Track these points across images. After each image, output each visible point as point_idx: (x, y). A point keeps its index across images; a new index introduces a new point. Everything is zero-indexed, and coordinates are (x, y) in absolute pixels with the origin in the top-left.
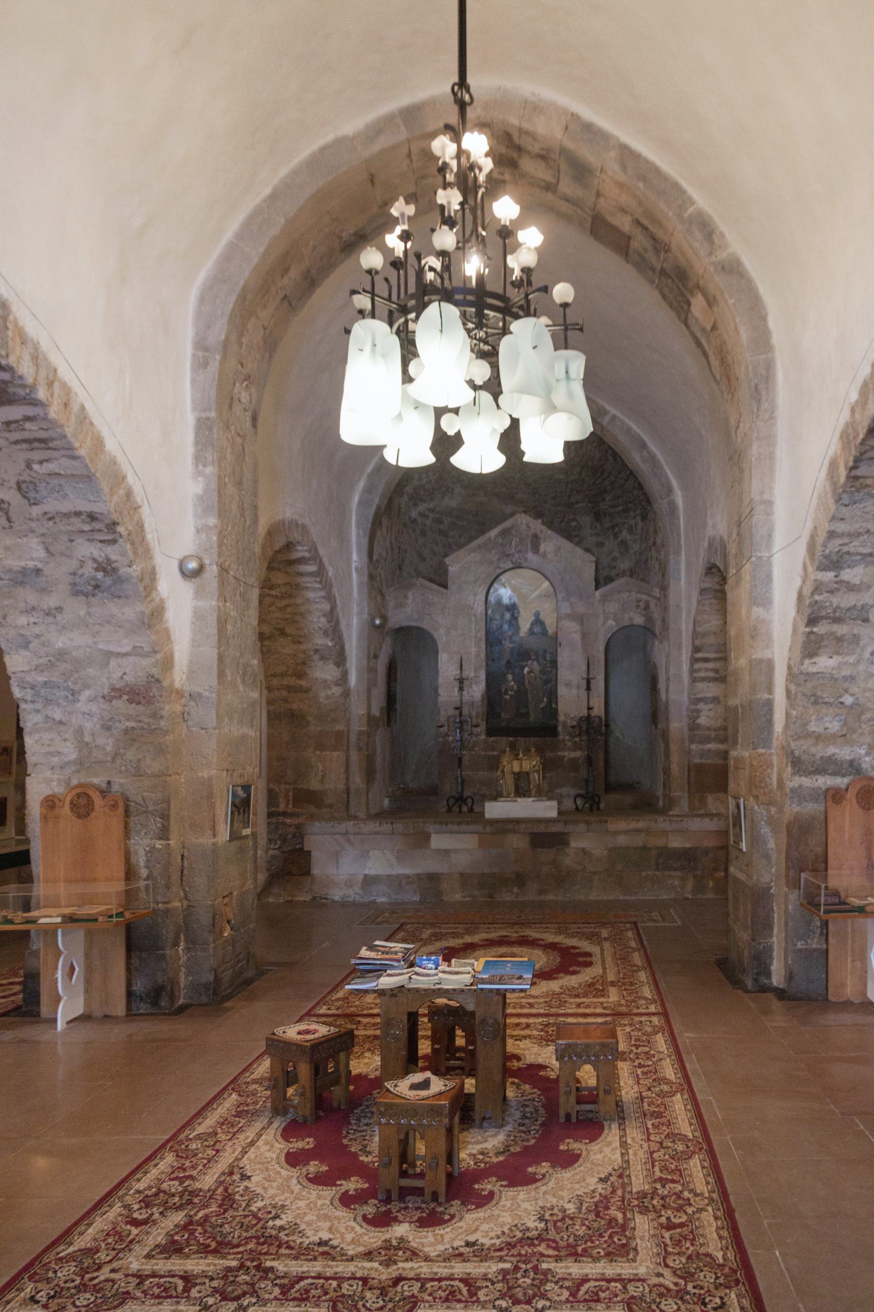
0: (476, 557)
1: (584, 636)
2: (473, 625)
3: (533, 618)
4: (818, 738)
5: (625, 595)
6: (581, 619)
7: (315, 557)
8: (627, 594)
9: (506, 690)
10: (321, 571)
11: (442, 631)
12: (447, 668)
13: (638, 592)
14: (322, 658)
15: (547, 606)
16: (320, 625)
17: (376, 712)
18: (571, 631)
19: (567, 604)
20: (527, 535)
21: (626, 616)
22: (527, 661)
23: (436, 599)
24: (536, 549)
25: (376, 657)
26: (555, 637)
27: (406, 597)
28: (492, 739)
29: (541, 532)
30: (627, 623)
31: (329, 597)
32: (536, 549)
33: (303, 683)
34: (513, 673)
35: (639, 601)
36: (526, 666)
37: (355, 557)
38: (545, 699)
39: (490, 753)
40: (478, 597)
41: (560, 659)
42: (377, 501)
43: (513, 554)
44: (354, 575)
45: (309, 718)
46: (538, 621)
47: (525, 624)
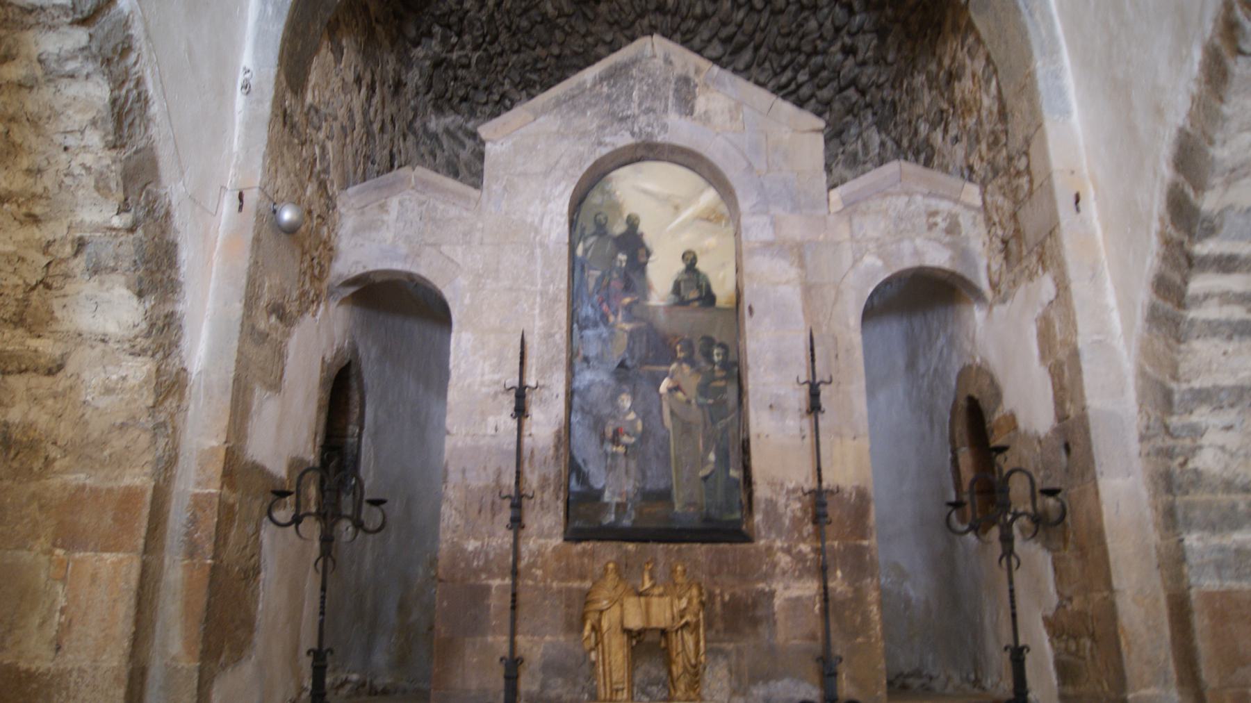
0: (550, 123)
1: (808, 290)
2: (539, 267)
3: (681, 266)
5: (901, 201)
6: (798, 253)
8: (905, 199)
9: (617, 433)
11: (463, 281)
12: (475, 364)
13: (930, 195)
14: (96, 270)
15: (711, 241)
16: (89, 159)
18: (774, 288)
19: (764, 219)
20: (666, 80)
21: (906, 246)
22: (669, 364)
23: (453, 212)
27: (383, 208)
28: (580, 547)
29: (698, 71)
30: (908, 263)
32: (686, 104)
33: (47, 347)
34: (634, 395)
35: (934, 214)
36: (666, 374)
37: (247, 59)
38: (712, 457)
39: (576, 584)
40: (552, 206)
43: (635, 117)
45: (54, 452)
46: (693, 287)
47: (662, 274)
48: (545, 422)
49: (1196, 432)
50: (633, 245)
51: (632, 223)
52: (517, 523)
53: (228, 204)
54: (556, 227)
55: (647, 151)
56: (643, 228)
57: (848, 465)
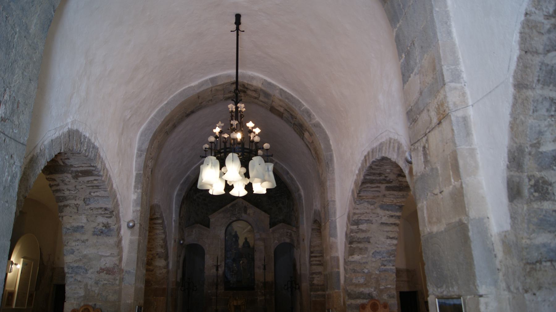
4: (356, 285)
7: (162, 217)
10: (163, 223)
12: (209, 261)
17: (179, 280)
18: (260, 245)
24: (245, 212)
25: (180, 256)
26: (253, 248)
31: (165, 233)
32: (245, 212)
41: (255, 257)
42: (184, 194)
44: (173, 223)
46: (246, 242)
47: (241, 242)
48: (221, 271)
49: (313, 278)
50: (236, 237)
51: (236, 232)
52: (217, 288)
53: (173, 242)
54: (222, 236)
55: (238, 220)
56: (238, 233)
57: (270, 277)
